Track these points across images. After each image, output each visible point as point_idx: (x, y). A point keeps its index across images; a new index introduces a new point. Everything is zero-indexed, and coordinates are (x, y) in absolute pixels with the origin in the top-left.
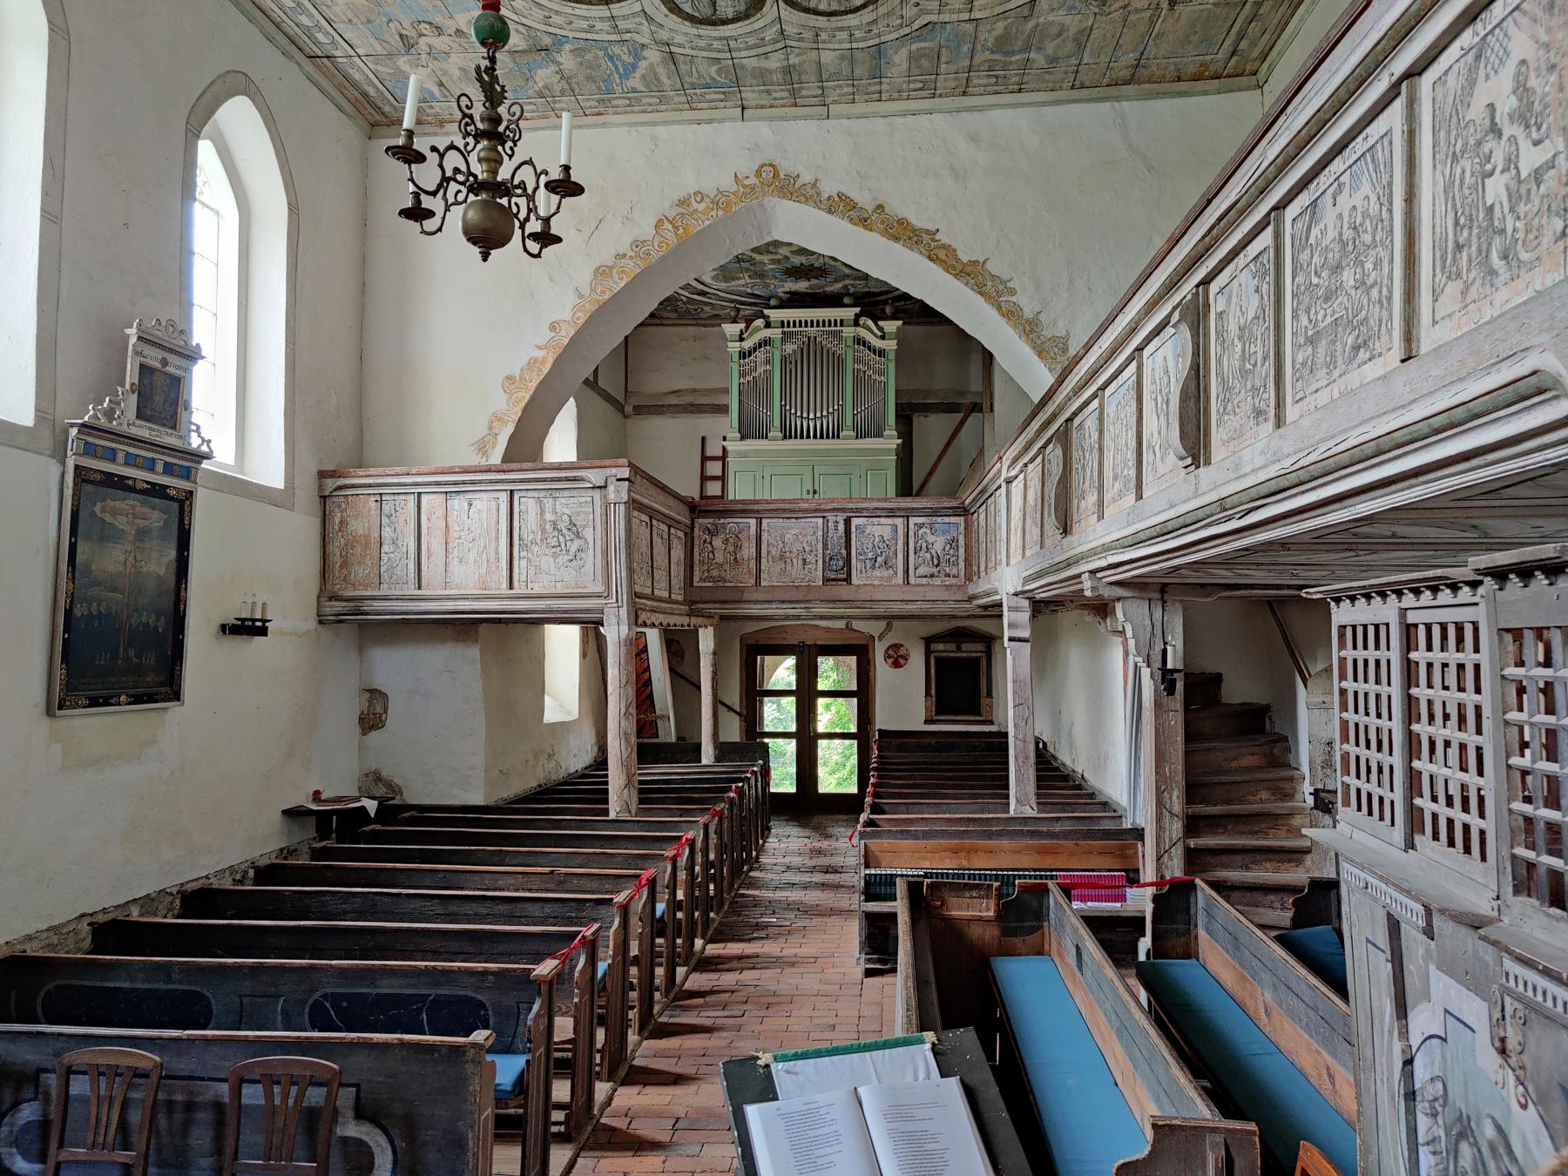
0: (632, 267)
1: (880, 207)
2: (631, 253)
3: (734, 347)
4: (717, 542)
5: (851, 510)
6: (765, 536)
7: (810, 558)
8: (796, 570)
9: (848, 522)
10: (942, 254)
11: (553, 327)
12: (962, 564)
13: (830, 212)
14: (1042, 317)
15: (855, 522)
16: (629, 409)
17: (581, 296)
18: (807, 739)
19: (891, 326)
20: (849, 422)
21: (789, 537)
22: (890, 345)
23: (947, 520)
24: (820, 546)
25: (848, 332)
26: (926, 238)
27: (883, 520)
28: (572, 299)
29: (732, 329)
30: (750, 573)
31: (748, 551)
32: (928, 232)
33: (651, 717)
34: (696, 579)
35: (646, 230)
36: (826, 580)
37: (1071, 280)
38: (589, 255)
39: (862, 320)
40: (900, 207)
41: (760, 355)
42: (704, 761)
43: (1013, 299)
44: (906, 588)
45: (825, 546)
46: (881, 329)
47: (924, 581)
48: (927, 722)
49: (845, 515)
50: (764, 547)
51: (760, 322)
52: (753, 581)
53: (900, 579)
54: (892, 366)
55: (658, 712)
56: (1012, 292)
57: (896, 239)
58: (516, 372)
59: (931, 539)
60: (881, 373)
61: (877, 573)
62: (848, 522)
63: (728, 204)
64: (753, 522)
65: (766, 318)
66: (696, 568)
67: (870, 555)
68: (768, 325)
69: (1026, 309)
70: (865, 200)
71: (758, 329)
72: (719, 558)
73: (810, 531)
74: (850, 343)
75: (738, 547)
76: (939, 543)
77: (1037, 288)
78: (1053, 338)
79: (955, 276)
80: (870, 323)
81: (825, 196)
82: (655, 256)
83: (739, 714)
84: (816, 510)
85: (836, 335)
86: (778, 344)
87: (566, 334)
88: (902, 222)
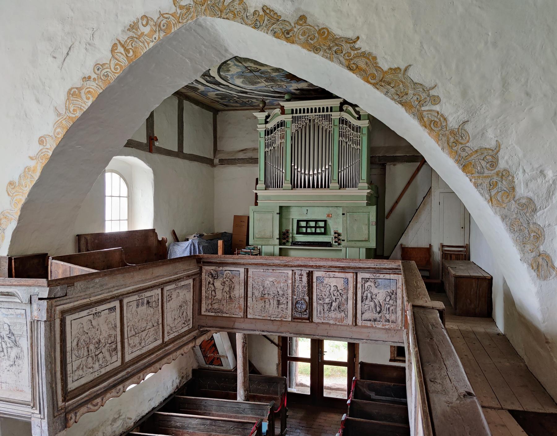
0: (96, 88)
1: (303, 18)
2: (94, 76)
3: (261, 128)
4: (218, 284)
5: (312, 266)
6: (250, 281)
7: (283, 300)
9: (310, 275)
10: (362, 63)
11: (41, 141)
12: (399, 313)
13: (255, 27)
14: (469, 128)
15: (316, 274)
16: (216, 161)
17: (59, 115)
18: (317, 362)
20: (336, 177)
21: (267, 283)
23: (387, 276)
24: (290, 291)
25: (336, 115)
26: (346, 47)
27: (337, 274)
28: (52, 118)
30: (240, 308)
31: (239, 291)
32: (348, 40)
33: (216, 356)
34: (203, 309)
35: (103, 54)
36: (294, 318)
37: (505, 84)
38: (63, 78)
40: (323, 15)
41: (277, 134)
42: (238, 398)
43: (437, 108)
44: (354, 329)
45: (293, 292)
47: (369, 324)
48: (391, 360)
49: (308, 270)
50: (250, 290)
52: (241, 314)
53: (350, 320)
55: (220, 354)
56: (436, 100)
57: (316, 49)
58: (16, 178)
60: (358, 143)
61: (332, 314)
62: (310, 275)
63: (168, 25)
64: (242, 270)
65: (282, 108)
66: (204, 302)
67: (327, 301)
69: (450, 119)
70: (286, 10)
71: (276, 115)
72: (219, 296)
73: (282, 279)
74: (337, 123)
75: (231, 289)
76: (381, 295)
77: (464, 94)
78: (481, 151)
79: (374, 85)
81: (252, 10)
82: (113, 77)
83: (278, 345)
84: (286, 266)
85: (328, 118)
86: (289, 125)
87: (51, 146)
88: (324, 33)
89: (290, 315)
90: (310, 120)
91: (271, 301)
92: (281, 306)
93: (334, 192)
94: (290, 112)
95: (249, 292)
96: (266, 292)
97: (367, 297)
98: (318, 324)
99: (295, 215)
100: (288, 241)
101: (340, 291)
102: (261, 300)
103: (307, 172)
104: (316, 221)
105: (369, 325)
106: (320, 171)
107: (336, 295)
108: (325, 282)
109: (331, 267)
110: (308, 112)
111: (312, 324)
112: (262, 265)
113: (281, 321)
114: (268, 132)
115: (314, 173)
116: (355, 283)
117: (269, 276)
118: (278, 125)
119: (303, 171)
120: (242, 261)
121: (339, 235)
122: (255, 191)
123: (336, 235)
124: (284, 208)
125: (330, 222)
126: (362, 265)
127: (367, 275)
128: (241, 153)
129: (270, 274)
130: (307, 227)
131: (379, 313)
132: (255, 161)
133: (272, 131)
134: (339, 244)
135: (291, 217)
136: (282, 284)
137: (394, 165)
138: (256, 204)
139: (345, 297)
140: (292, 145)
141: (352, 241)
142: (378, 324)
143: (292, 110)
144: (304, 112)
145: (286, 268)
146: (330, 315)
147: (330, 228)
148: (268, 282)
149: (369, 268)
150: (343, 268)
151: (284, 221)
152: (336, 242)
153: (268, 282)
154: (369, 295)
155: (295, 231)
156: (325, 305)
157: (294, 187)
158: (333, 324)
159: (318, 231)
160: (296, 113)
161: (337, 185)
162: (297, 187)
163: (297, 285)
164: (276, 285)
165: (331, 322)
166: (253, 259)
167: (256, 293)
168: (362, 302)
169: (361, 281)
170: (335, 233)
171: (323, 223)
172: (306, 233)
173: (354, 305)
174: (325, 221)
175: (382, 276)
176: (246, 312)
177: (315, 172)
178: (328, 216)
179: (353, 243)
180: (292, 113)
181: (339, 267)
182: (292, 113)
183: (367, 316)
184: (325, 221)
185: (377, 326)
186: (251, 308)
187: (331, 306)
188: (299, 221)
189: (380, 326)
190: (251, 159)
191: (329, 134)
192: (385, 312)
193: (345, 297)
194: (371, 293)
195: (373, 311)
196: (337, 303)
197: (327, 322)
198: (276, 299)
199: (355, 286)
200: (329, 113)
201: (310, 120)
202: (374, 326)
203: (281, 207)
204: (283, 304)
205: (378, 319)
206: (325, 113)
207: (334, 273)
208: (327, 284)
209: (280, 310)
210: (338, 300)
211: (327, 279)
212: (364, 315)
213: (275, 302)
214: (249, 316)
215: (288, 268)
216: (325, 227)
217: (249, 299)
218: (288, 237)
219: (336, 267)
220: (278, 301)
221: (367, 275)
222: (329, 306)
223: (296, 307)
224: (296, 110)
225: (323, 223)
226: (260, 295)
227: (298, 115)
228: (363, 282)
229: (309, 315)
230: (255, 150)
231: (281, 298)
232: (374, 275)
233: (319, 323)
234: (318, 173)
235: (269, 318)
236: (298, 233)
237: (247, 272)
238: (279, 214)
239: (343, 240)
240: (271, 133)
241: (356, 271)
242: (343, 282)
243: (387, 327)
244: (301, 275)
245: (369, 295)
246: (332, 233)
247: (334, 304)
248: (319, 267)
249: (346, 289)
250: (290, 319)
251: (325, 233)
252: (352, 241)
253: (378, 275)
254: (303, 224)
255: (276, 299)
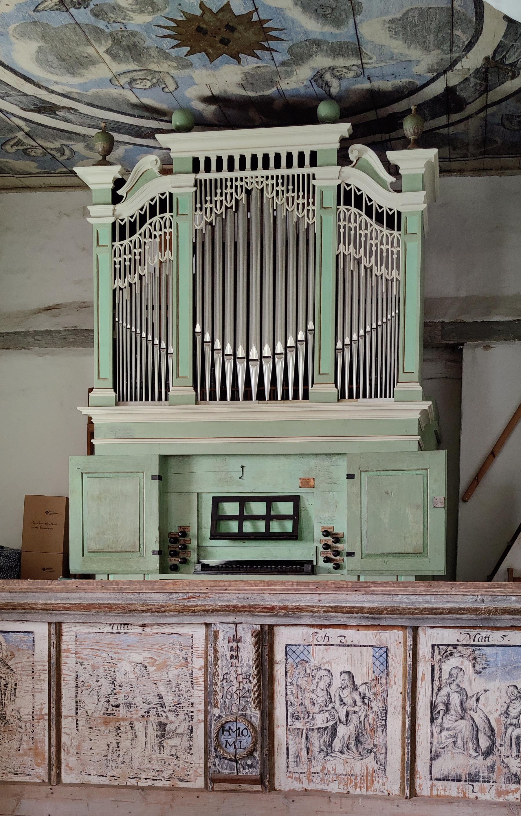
3: (102, 216)
5: (271, 610)
6: (69, 664)
7: (176, 722)
8: (141, 754)
9: (264, 638)
15: (284, 637)
19: (416, 161)
21: (125, 670)
22: (411, 203)
27: (352, 635)
29: (99, 178)
30: (36, 751)
36: (213, 780)
39: (355, 151)
46: (393, 170)
47: (453, 789)
51: (150, 162)
52: (42, 772)
53: (393, 781)
54: (414, 248)
59: (473, 684)
61: (337, 764)
62: (264, 638)
64: (41, 630)
67: (320, 721)
68: (166, 171)
73: (175, 656)
74: (330, 199)
80: (371, 156)
84: (184, 611)
85: (304, 186)
89: (202, 771)
90: (249, 193)
91: (139, 727)
92: (171, 742)
93: (323, 407)
94: (190, 167)
95: (64, 702)
96: (121, 699)
97: (448, 704)
98: (290, 795)
99: (208, 481)
100: (185, 561)
101: (363, 689)
102: (106, 723)
103: (241, 352)
104: (270, 500)
105: (454, 794)
106: (280, 348)
107: (348, 700)
108: (314, 661)
109: (335, 609)
110: (243, 168)
111: (273, 795)
112: (108, 609)
113: (173, 788)
114: (122, 228)
115: (264, 355)
116: (410, 661)
117: (130, 647)
118: (153, 208)
119: (229, 350)
120: (40, 599)
121: (337, 539)
122: (85, 411)
123: (329, 540)
124: (172, 462)
125: (311, 504)
126: (434, 603)
127: (449, 636)
128: (44, 316)
129: (133, 640)
130: (241, 518)
131: (487, 754)
132: (83, 338)
133: (132, 225)
134: (337, 567)
135: (196, 489)
136: (173, 673)
137: (487, 348)
138: (91, 450)
139: (376, 706)
140: (194, 276)
141: (377, 555)
142: (483, 791)
143: (196, 161)
144: (231, 168)
145: (187, 619)
146: (329, 766)
147: (309, 519)
148: (127, 667)
149: (458, 611)
150: (372, 611)
151: (174, 500)
152: (327, 560)
153: (127, 667)
154: (455, 699)
155: (207, 531)
156: (314, 737)
157: (203, 398)
158: (340, 795)
159: (275, 527)
160: (208, 169)
161: (334, 391)
162: (213, 397)
163: (221, 672)
164: (155, 676)
165: (334, 788)
166: (77, 590)
167: (90, 704)
168: (433, 720)
169: (428, 656)
170: (327, 533)
171: (291, 504)
172: (241, 537)
173: (408, 733)
174: (296, 500)
175: (496, 637)
176: (55, 763)
177: (267, 351)
178: (306, 483)
179: (379, 560)
180: (196, 169)
181: (360, 610)
182: (196, 169)
183: (447, 764)
184: (296, 500)
185: (482, 797)
186: (73, 751)
187: (333, 736)
188: (217, 501)
189: (490, 796)
190: (75, 331)
191: (306, 241)
192: (504, 751)
193: (376, 706)
194: (461, 691)
195: (466, 749)
196: (352, 727)
197: (319, 787)
198: (153, 719)
199: (409, 669)
200: (307, 170)
201: (249, 193)
202: (472, 796)
203: (164, 459)
204: (176, 734)
205: (484, 773)
206: (295, 171)
207: (342, 632)
208: (318, 669)
209: (166, 754)
210: (354, 718)
211: (319, 652)
212: (437, 763)
213: (152, 731)
214: (65, 778)
215: (194, 620)
216: (296, 517)
217: (64, 723)
218: (185, 547)
219: (350, 610)
220: (162, 726)
221: (449, 636)
222: (326, 737)
223: (219, 745)
224: (208, 160)
225: (291, 504)
226: (101, 707)
227: (214, 175)
228: (437, 657)
229: (263, 768)
230: (85, 306)
231: (172, 717)
232: (473, 633)
233: (294, 792)
234: (274, 353)
235: (133, 782)
236: (216, 535)
237: (59, 634)
238: (160, 478)
239: (350, 554)
240: (133, 232)
241: (413, 622)
242: (371, 660)
243: (511, 798)
244: (236, 639)
245: (455, 699)
246: (318, 534)
247: (342, 730)
248: (298, 611)
249: (382, 682)
250: (200, 783)
251: (294, 536)
252: (377, 555)
253: (484, 633)
254: (231, 509)
255: (153, 719)
